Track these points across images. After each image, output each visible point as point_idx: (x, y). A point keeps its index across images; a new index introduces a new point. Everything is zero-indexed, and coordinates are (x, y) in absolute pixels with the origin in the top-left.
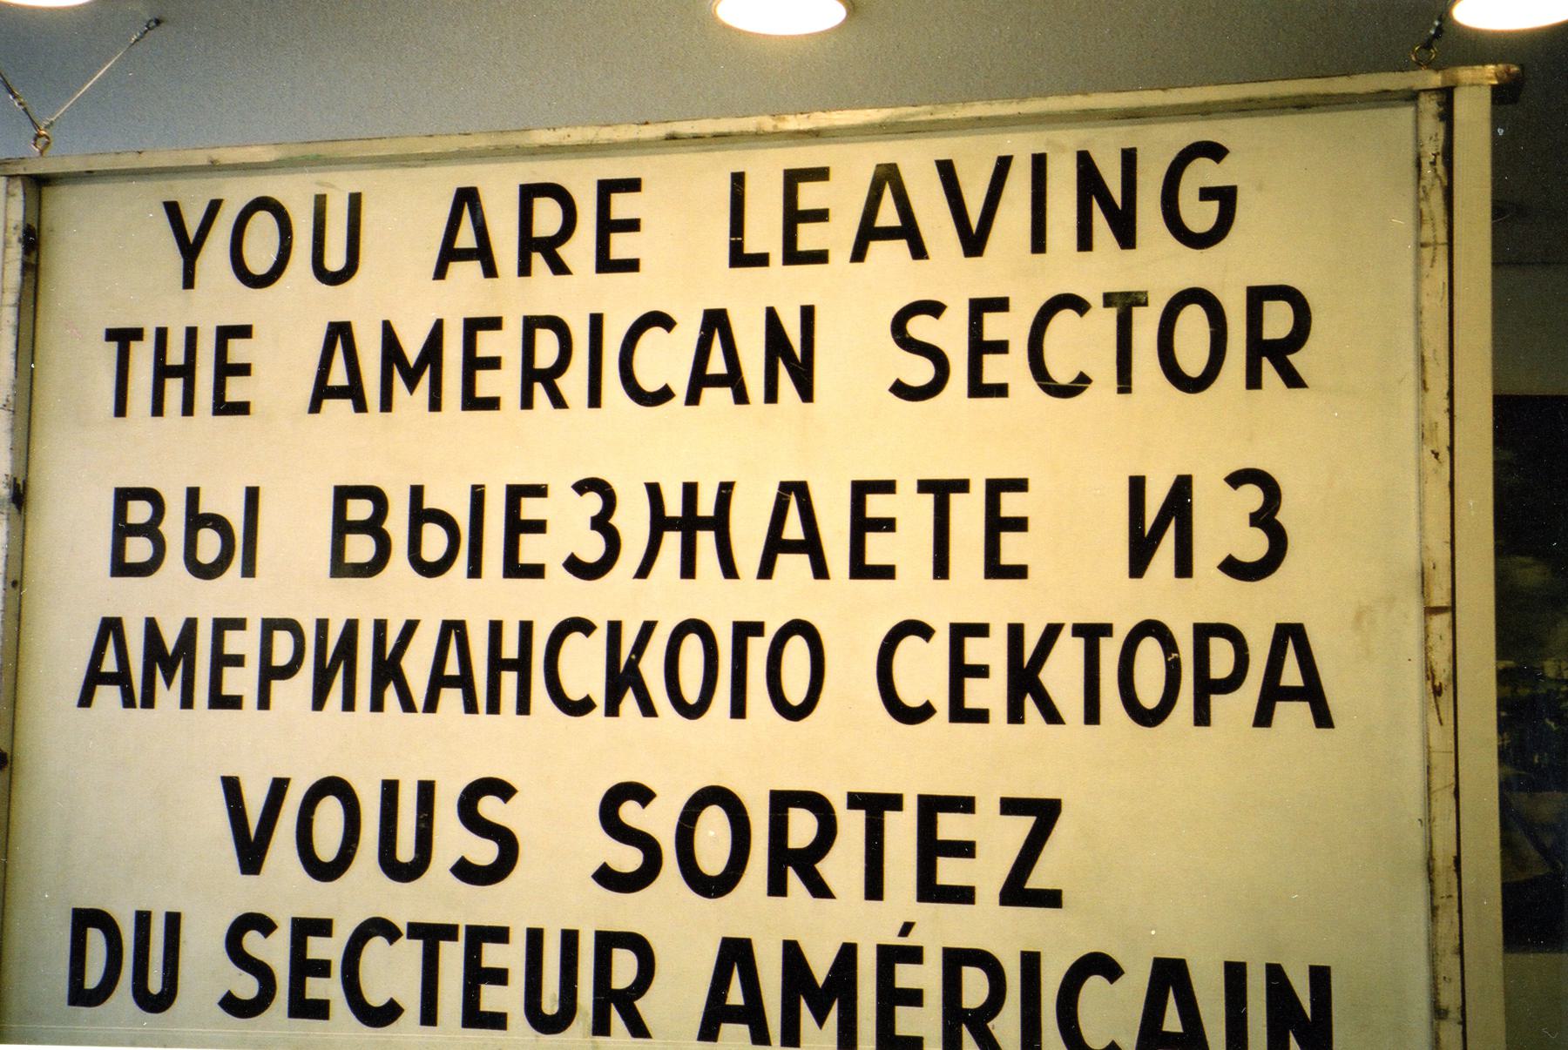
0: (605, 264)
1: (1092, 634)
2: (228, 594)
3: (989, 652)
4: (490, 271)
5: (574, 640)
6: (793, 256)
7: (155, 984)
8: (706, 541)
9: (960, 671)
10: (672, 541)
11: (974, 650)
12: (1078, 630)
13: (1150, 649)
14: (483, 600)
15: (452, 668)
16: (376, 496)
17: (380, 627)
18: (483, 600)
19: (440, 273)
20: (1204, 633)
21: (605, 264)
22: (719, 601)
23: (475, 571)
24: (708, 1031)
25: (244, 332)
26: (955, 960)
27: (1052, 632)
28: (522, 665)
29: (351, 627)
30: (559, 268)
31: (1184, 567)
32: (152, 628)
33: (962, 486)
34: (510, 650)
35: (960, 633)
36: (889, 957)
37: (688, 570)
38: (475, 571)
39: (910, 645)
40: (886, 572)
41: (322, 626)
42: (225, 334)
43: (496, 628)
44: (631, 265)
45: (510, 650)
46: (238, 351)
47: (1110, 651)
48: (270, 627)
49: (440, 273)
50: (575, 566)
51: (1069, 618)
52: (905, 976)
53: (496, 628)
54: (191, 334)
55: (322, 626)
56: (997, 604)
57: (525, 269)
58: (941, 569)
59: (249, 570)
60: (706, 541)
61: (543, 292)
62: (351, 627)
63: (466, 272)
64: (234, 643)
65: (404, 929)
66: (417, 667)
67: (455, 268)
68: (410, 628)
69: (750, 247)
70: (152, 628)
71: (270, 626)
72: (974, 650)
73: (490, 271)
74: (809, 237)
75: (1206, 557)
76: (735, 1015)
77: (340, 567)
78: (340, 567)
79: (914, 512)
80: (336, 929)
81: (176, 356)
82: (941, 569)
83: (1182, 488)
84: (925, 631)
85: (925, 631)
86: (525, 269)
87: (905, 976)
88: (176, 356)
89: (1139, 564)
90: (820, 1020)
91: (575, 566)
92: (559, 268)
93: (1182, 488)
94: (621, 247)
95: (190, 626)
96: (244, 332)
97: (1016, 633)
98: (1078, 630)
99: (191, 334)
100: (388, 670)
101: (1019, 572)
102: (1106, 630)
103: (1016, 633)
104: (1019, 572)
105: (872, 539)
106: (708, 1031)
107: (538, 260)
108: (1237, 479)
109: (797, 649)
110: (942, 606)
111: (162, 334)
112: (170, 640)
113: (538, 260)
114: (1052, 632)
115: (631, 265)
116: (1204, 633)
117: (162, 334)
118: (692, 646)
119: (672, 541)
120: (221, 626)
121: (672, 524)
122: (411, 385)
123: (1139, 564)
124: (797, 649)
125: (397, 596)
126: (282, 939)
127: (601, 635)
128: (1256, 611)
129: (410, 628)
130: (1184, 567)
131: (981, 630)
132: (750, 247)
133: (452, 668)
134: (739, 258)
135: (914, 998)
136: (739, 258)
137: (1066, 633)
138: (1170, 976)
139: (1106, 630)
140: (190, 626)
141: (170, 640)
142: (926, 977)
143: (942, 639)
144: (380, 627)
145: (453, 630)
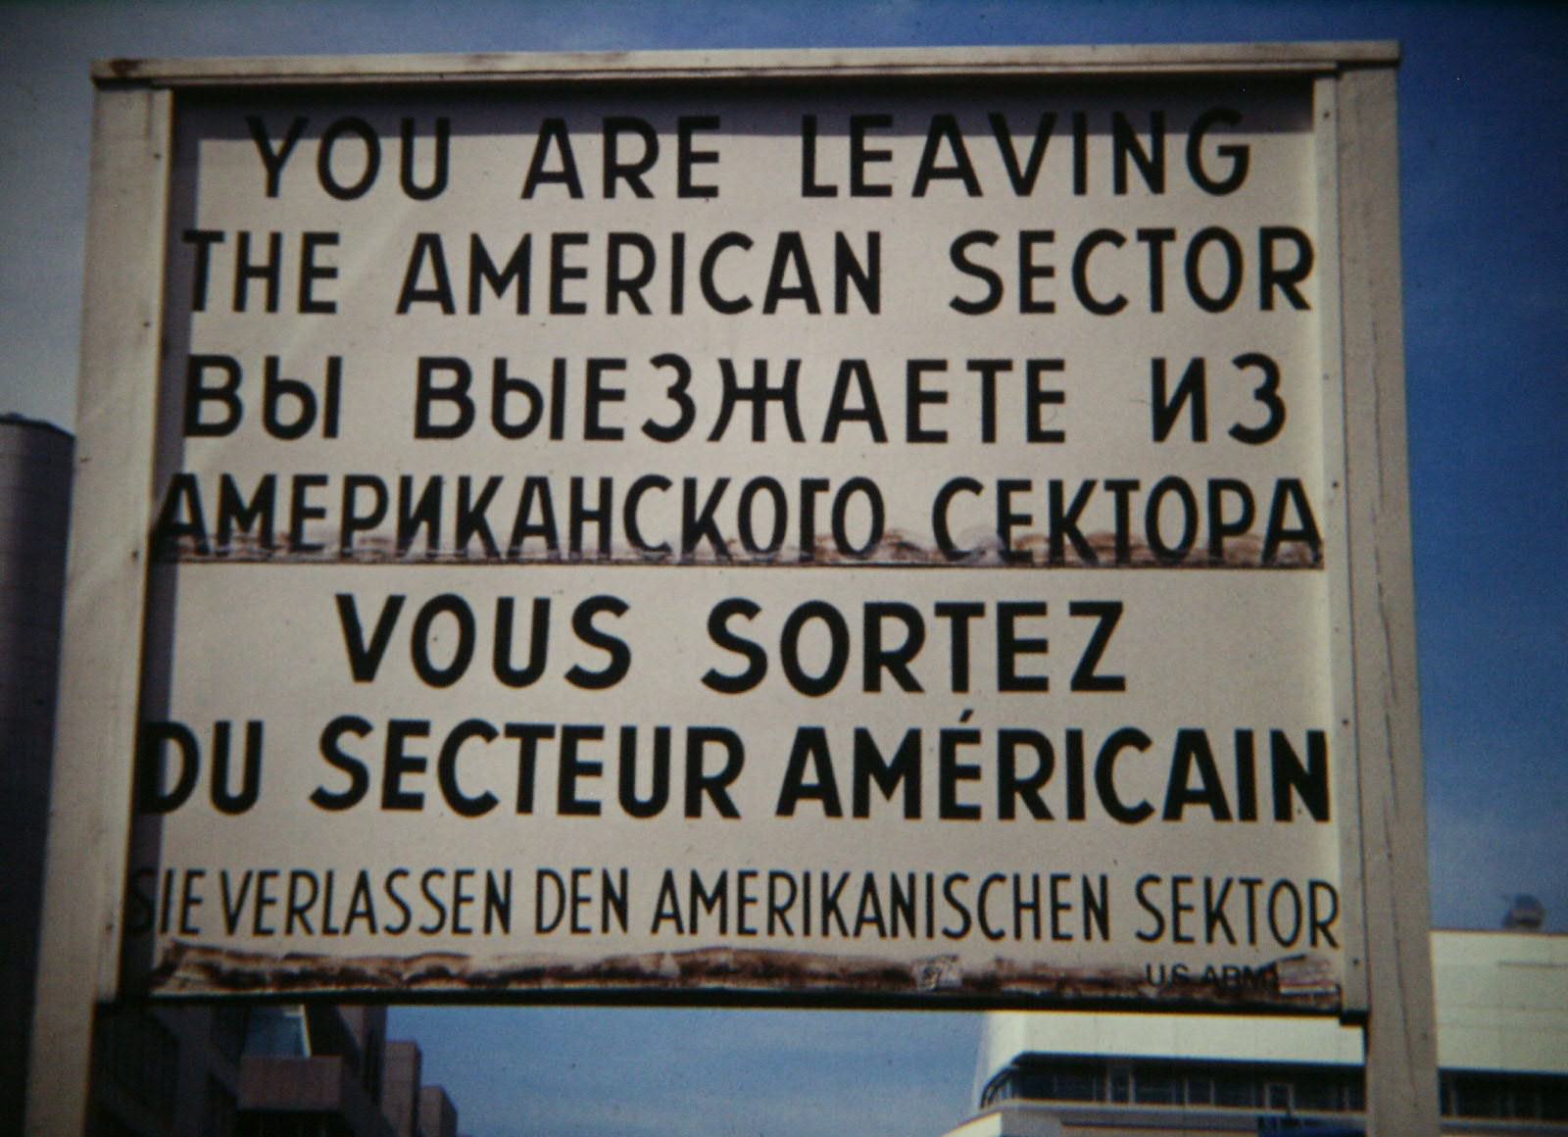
0: (686, 190)
1: (1122, 489)
2: (311, 452)
3: (1034, 503)
4: (576, 192)
5: (651, 495)
6: (859, 188)
7: (235, 787)
8: (775, 410)
9: (1007, 519)
10: (743, 410)
11: (1019, 503)
12: (1110, 485)
13: (1172, 501)
14: (565, 459)
15: (536, 518)
16: (461, 368)
17: (464, 483)
18: (565, 459)
19: (528, 192)
20: (1216, 487)
21: (686, 190)
22: (789, 462)
23: (557, 432)
24: (785, 808)
25: (331, 239)
26: (1009, 740)
27: (1087, 487)
28: (603, 516)
29: (435, 484)
30: (642, 192)
31: (1200, 433)
32: (227, 485)
33: (1006, 365)
34: (591, 501)
35: (1006, 488)
36: (950, 739)
37: (759, 433)
38: (557, 432)
39: (962, 498)
40: (940, 437)
41: (406, 483)
42: (311, 240)
43: (577, 485)
44: (710, 192)
45: (591, 501)
46: (322, 256)
47: (1138, 502)
48: (352, 483)
49: (528, 192)
50: (652, 430)
51: (1101, 476)
52: (964, 755)
53: (577, 485)
54: (276, 240)
55: (406, 483)
56: (1042, 464)
57: (609, 191)
58: (989, 434)
59: (331, 430)
60: (775, 410)
61: (626, 211)
62: (435, 484)
63: (552, 193)
64: (313, 497)
65: (500, 728)
66: (501, 518)
67: (542, 189)
68: (494, 483)
69: (820, 180)
70: (227, 485)
71: (352, 483)
72: (1019, 503)
73: (576, 192)
74: (873, 174)
75: (1218, 425)
76: (810, 793)
77: (424, 430)
78: (424, 430)
79: (964, 387)
80: (434, 729)
81: (259, 257)
82: (989, 434)
83: (1195, 376)
84: (975, 487)
85: (975, 487)
86: (609, 191)
87: (964, 755)
88: (259, 257)
89: (1161, 430)
90: (888, 792)
91: (652, 430)
92: (642, 192)
93: (1195, 376)
94: (700, 174)
95: (268, 485)
96: (331, 239)
97: (1056, 488)
98: (1110, 485)
99: (276, 240)
100: (472, 521)
101: (1057, 437)
102: (1134, 485)
103: (1056, 488)
104: (1057, 437)
105: (926, 409)
106: (785, 808)
107: (622, 184)
108: (1243, 362)
109: (859, 502)
110: (990, 465)
111: (244, 239)
112: (247, 493)
113: (622, 184)
114: (1087, 487)
115: (710, 192)
116: (1216, 487)
117: (244, 239)
118: (763, 500)
119: (743, 410)
120: (301, 483)
121: (744, 395)
122: (500, 285)
123: (1161, 430)
124: (859, 502)
125: (480, 454)
126: (379, 738)
127: (677, 491)
128: (1260, 468)
129: (494, 483)
130: (1200, 433)
131: (1025, 486)
132: (820, 180)
133: (536, 518)
134: (810, 189)
135: (973, 773)
136: (810, 189)
137: (1099, 488)
138: (1192, 743)
139: (1134, 485)
140: (268, 485)
141: (247, 493)
142: (983, 755)
143: (990, 493)
144: (464, 483)
145: (535, 486)
